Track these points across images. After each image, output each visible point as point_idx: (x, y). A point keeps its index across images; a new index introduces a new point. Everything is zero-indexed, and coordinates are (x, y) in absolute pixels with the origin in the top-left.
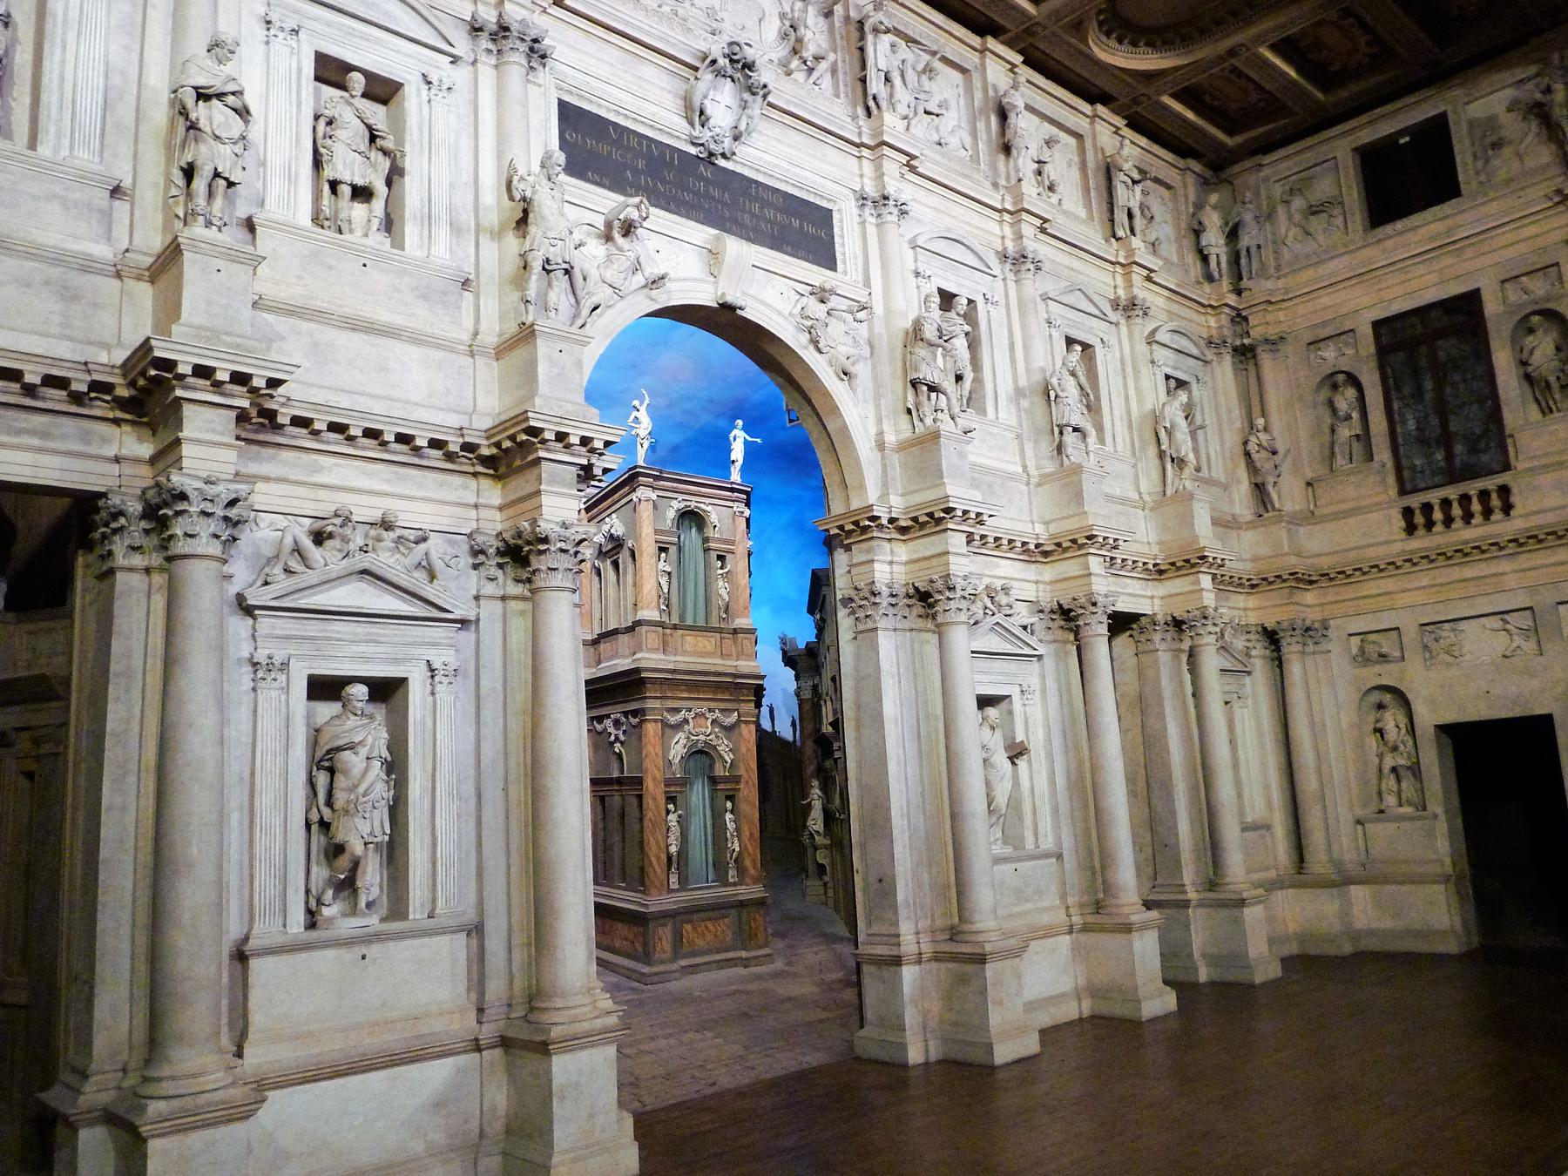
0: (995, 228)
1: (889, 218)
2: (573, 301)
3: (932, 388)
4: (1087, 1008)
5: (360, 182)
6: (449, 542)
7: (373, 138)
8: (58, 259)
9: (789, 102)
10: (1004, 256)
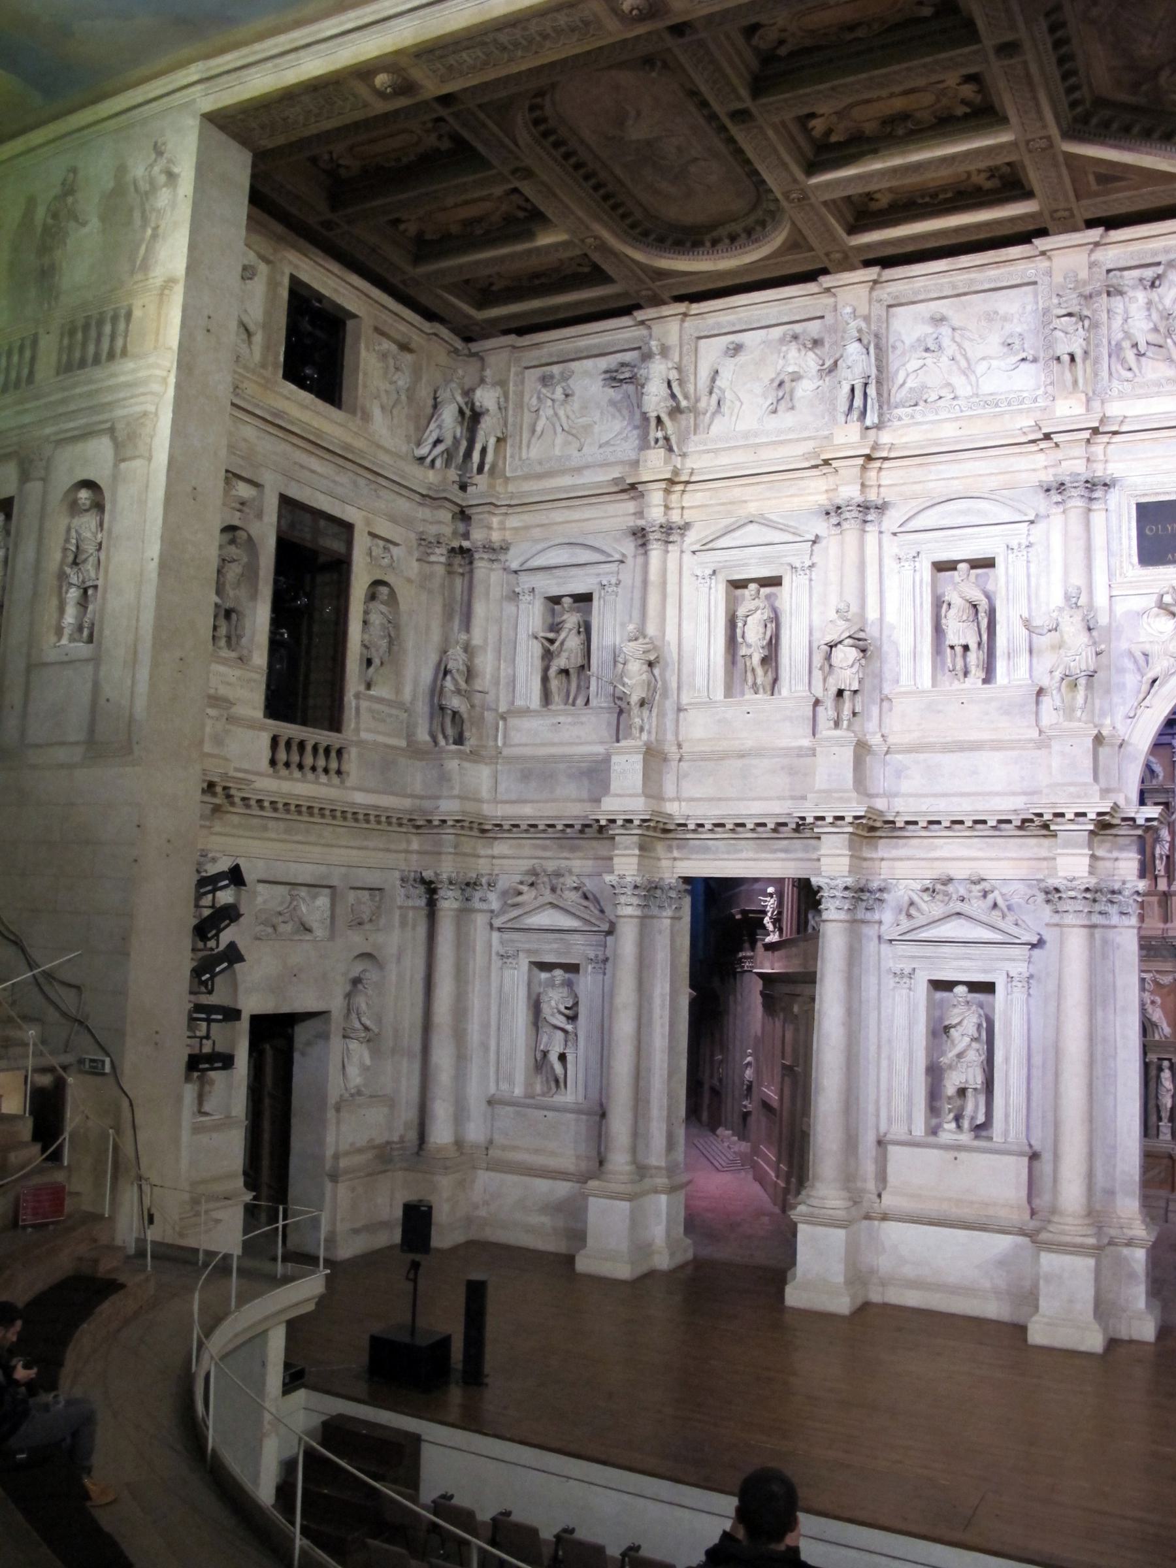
2: (1139, 678)
5: (964, 643)
6: (1030, 886)
7: (975, 606)
8: (787, 752)
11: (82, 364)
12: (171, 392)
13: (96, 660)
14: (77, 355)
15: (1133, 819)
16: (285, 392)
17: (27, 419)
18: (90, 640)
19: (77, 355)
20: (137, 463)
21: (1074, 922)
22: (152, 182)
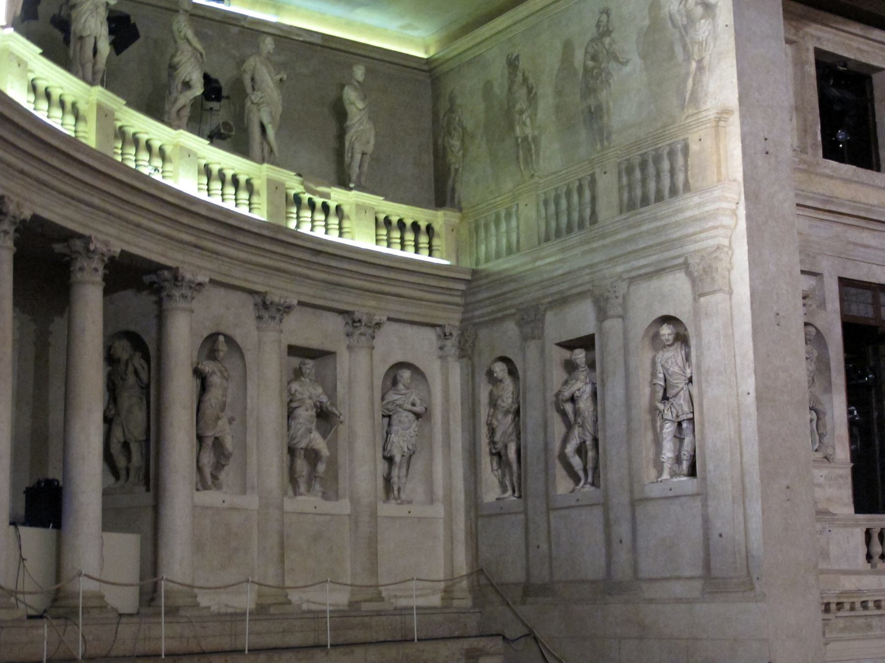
11: (645, 201)
12: (742, 224)
13: (702, 495)
14: (638, 192)
16: (828, 171)
17: (597, 258)
18: (692, 472)
19: (638, 192)
20: (719, 297)
22: (689, 15)
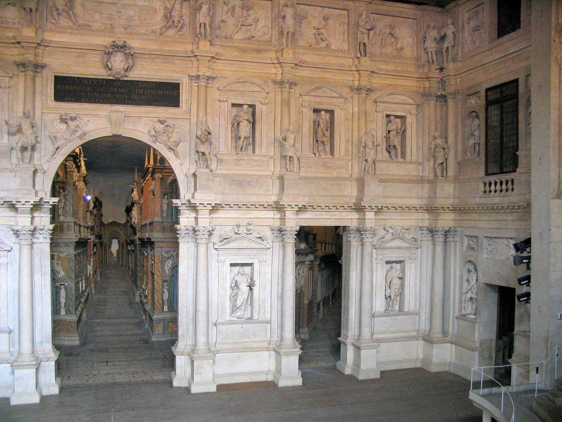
0: (274, 71)
1: (200, 83)
3: (204, 154)
4: (270, 378)
6: (7, 227)
9: (150, 51)
10: (275, 82)
15: (48, 202)
21: (25, 243)
